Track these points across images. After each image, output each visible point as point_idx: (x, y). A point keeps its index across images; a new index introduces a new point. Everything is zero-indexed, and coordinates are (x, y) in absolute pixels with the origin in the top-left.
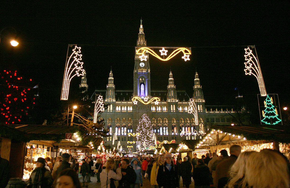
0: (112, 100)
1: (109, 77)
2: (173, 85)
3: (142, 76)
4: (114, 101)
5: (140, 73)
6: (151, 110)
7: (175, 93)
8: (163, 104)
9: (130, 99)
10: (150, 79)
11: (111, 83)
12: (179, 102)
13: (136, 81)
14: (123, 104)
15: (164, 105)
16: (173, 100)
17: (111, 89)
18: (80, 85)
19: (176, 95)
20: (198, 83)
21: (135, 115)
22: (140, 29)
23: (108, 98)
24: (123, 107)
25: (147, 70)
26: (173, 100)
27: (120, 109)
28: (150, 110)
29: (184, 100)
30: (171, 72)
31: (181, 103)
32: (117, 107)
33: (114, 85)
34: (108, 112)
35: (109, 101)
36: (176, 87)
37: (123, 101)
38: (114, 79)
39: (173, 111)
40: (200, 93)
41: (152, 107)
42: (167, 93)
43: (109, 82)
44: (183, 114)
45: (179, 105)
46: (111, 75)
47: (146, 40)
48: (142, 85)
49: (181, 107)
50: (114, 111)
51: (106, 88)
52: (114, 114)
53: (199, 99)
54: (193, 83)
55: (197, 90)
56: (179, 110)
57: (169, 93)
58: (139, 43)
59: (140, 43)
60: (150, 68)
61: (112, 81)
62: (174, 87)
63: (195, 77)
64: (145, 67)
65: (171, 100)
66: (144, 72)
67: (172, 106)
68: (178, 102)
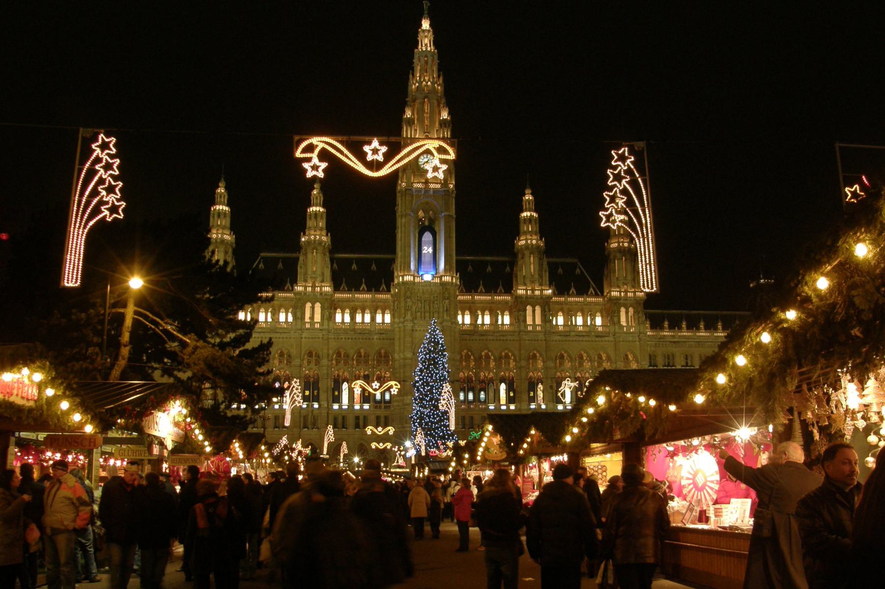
0: (321, 287)
1: (310, 205)
2: (536, 234)
3: (427, 203)
4: (327, 289)
6: (457, 323)
7: (541, 265)
8: (500, 302)
9: (384, 286)
10: (454, 211)
12: (554, 294)
13: (403, 220)
15: (503, 307)
16: (533, 290)
17: (316, 250)
19: (545, 271)
21: (400, 339)
23: (306, 281)
26: (533, 290)
27: (347, 319)
28: (452, 323)
29: (573, 290)
30: (528, 191)
31: (562, 299)
32: (339, 311)
34: (308, 329)
35: (309, 289)
36: (546, 243)
37: (358, 290)
39: (534, 325)
40: (629, 266)
41: (460, 312)
42: (513, 264)
43: (310, 223)
44: (568, 338)
45: (557, 306)
46: (317, 198)
48: (427, 237)
49: (560, 314)
50: (328, 325)
51: (297, 247)
52: (325, 337)
53: (626, 286)
55: (618, 255)
56: (554, 323)
57: (520, 262)
58: (417, 84)
59: (420, 83)
61: (319, 219)
62: (537, 242)
65: (527, 290)
67: (529, 309)
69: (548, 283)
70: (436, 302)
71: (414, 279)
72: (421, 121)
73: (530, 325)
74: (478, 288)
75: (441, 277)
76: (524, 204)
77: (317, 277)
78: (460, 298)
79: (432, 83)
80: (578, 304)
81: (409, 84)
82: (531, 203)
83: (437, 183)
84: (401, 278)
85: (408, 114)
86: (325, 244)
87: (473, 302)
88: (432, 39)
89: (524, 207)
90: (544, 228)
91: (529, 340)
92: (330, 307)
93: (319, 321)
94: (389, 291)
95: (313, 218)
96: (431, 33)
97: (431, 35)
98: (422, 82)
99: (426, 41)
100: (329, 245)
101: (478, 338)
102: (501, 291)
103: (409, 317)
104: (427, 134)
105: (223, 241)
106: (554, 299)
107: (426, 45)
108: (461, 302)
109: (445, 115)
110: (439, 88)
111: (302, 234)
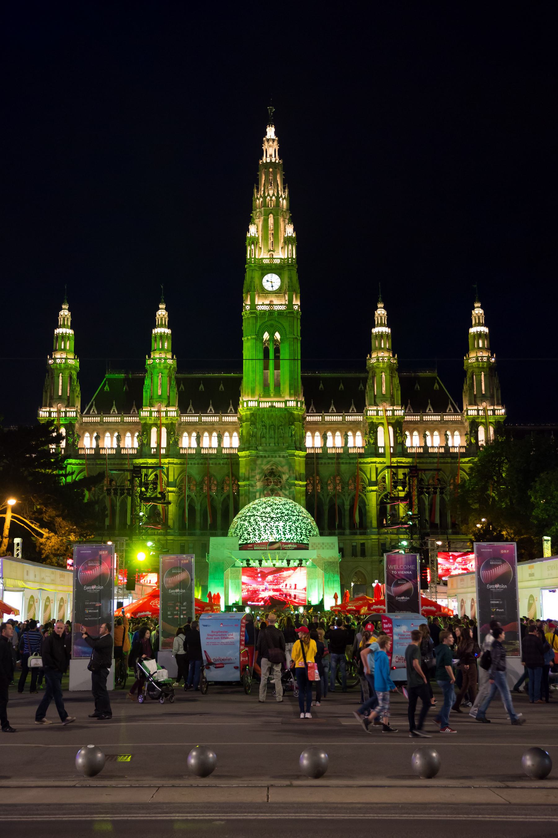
1: (155, 327)
2: (388, 350)
3: (272, 326)
5: (264, 313)
9: (231, 407)
14: (205, 423)
15: (355, 426)
17: (162, 373)
18: (51, 358)
20: (481, 345)
22: (266, 143)
24: (206, 434)
25: (291, 301)
30: (380, 305)
31: (418, 418)
33: (172, 358)
38: (172, 334)
42: (365, 381)
43: (154, 345)
47: (289, 188)
58: (261, 199)
59: (264, 198)
60: (299, 295)
63: (474, 322)
64: (278, 292)
66: (276, 308)
69: (400, 402)
70: (281, 427)
71: (259, 405)
73: (381, 447)
74: (329, 408)
75: (286, 402)
76: (376, 319)
77: (162, 402)
78: (308, 419)
79: (276, 197)
80: (435, 423)
81: (253, 199)
82: (383, 318)
83: (281, 305)
84: (245, 403)
85: (253, 230)
86: (171, 367)
87: (323, 422)
88: (277, 148)
93: (165, 446)
94: (236, 411)
95: (158, 339)
96: (276, 143)
97: (276, 146)
98: (266, 197)
99: (271, 151)
100: (174, 368)
101: (327, 461)
102: (353, 410)
104: (271, 252)
105: (67, 367)
106: (408, 418)
107: (271, 155)
108: (310, 423)
109: (290, 230)
110: (285, 201)
111: (147, 356)
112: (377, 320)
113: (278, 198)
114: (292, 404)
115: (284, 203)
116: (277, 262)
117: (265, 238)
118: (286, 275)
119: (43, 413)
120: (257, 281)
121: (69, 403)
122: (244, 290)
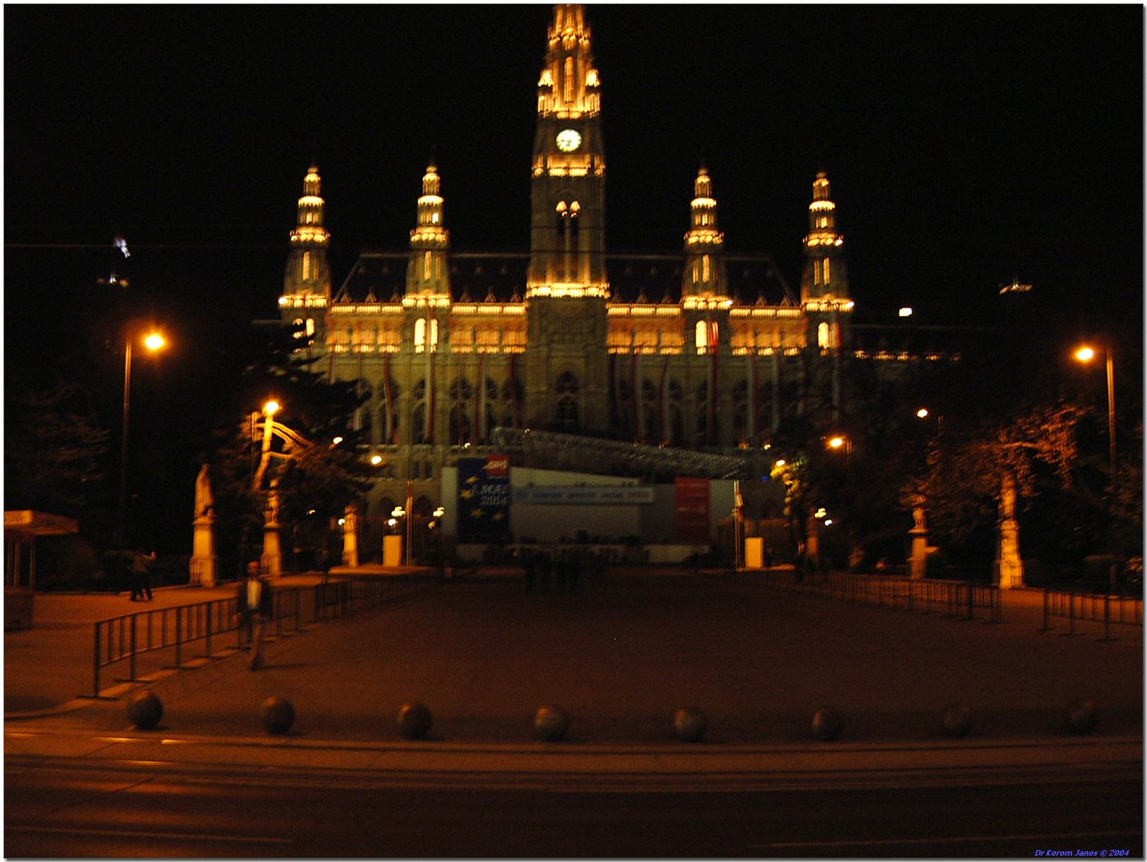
4: (443, 301)
5: (557, 178)
11: (430, 224)
23: (417, 292)
26: (706, 302)
31: (745, 312)
43: (422, 218)
54: (806, 224)
64: (578, 153)
68: (729, 310)
72: (562, 88)
85: (547, 78)
89: (696, 194)
90: (721, 220)
91: (698, 367)
92: (447, 322)
103: (543, 340)
109: (592, 79)
112: (698, 191)
113: (578, 37)
114: (594, 291)
115: (585, 43)
116: (575, 115)
117: (562, 88)
118: (587, 131)
119: (283, 301)
120: (550, 140)
121: (317, 291)
122: (536, 149)
